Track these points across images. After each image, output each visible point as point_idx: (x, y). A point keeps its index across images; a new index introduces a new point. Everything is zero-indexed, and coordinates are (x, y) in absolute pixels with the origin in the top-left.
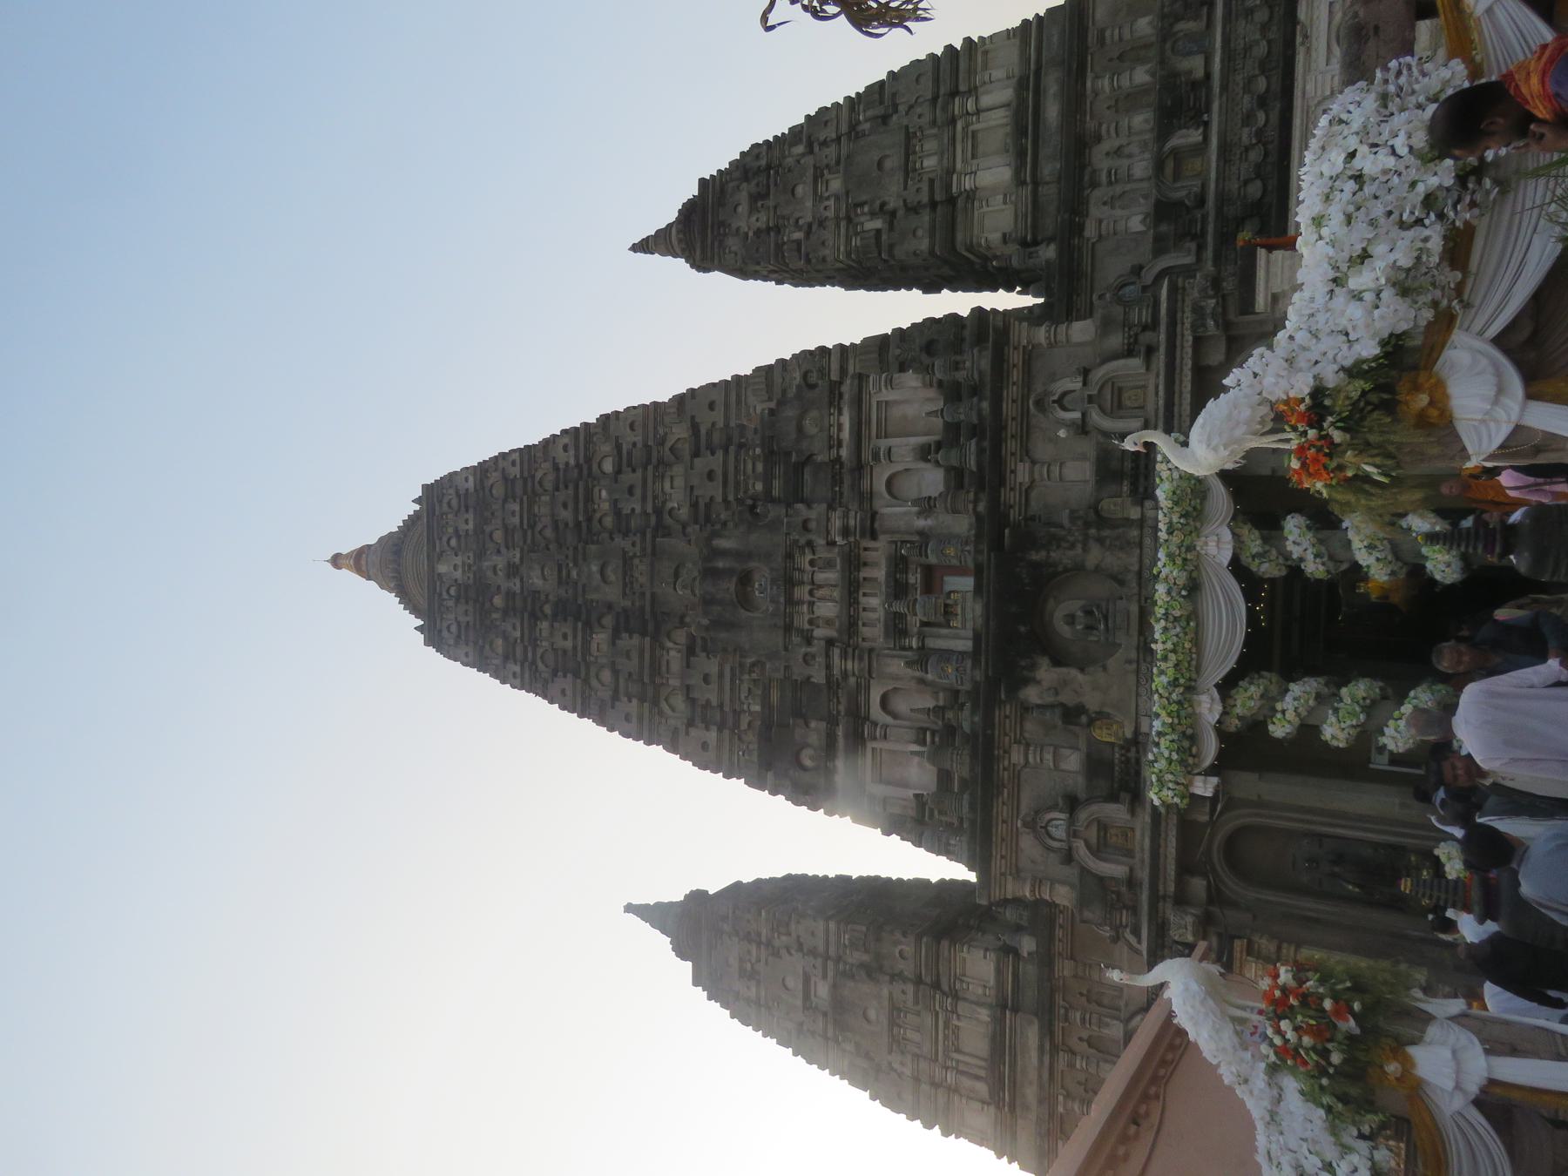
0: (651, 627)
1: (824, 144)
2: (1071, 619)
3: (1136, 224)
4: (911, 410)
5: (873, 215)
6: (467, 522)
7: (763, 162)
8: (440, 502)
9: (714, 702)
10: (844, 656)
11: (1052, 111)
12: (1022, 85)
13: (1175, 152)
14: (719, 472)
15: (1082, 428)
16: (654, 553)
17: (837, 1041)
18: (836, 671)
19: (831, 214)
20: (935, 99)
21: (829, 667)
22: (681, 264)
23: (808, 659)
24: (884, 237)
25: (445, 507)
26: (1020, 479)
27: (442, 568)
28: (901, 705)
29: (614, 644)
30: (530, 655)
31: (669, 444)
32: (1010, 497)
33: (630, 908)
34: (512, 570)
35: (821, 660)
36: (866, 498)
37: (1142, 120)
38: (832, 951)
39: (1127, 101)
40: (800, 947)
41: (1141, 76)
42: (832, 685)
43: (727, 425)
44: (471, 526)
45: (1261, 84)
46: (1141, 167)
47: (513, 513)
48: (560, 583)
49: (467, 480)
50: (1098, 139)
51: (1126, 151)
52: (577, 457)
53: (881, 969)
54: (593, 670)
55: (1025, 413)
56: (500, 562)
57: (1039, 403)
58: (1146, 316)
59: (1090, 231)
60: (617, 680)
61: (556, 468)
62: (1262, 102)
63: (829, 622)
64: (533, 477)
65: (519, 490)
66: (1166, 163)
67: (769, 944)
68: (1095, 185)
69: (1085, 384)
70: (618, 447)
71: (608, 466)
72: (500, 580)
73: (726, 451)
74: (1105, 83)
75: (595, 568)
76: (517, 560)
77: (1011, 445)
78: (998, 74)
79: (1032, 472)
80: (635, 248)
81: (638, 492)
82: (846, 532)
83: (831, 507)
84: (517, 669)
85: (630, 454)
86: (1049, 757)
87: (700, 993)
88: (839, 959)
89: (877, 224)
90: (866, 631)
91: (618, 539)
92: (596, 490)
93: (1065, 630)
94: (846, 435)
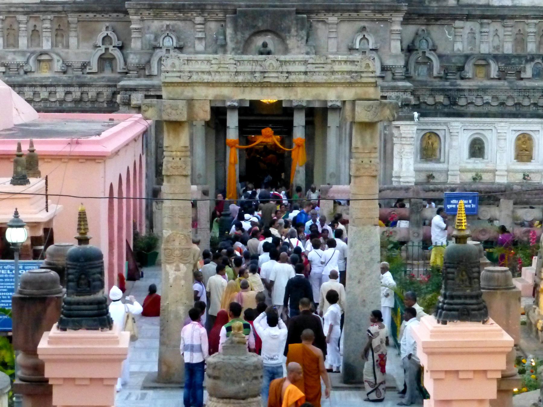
2: (265, 45)
3: (459, 46)
13: (488, 65)
26: (330, 19)
32: (322, 16)
37: (508, 48)
45: (510, 103)
46: (485, 49)
51: (496, 39)
55: (361, 20)
57: (364, 28)
58: (398, 76)
59: (458, 23)
62: (502, 104)
69: (371, 50)
77: (346, 15)
79: (333, 24)
86: (200, 35)
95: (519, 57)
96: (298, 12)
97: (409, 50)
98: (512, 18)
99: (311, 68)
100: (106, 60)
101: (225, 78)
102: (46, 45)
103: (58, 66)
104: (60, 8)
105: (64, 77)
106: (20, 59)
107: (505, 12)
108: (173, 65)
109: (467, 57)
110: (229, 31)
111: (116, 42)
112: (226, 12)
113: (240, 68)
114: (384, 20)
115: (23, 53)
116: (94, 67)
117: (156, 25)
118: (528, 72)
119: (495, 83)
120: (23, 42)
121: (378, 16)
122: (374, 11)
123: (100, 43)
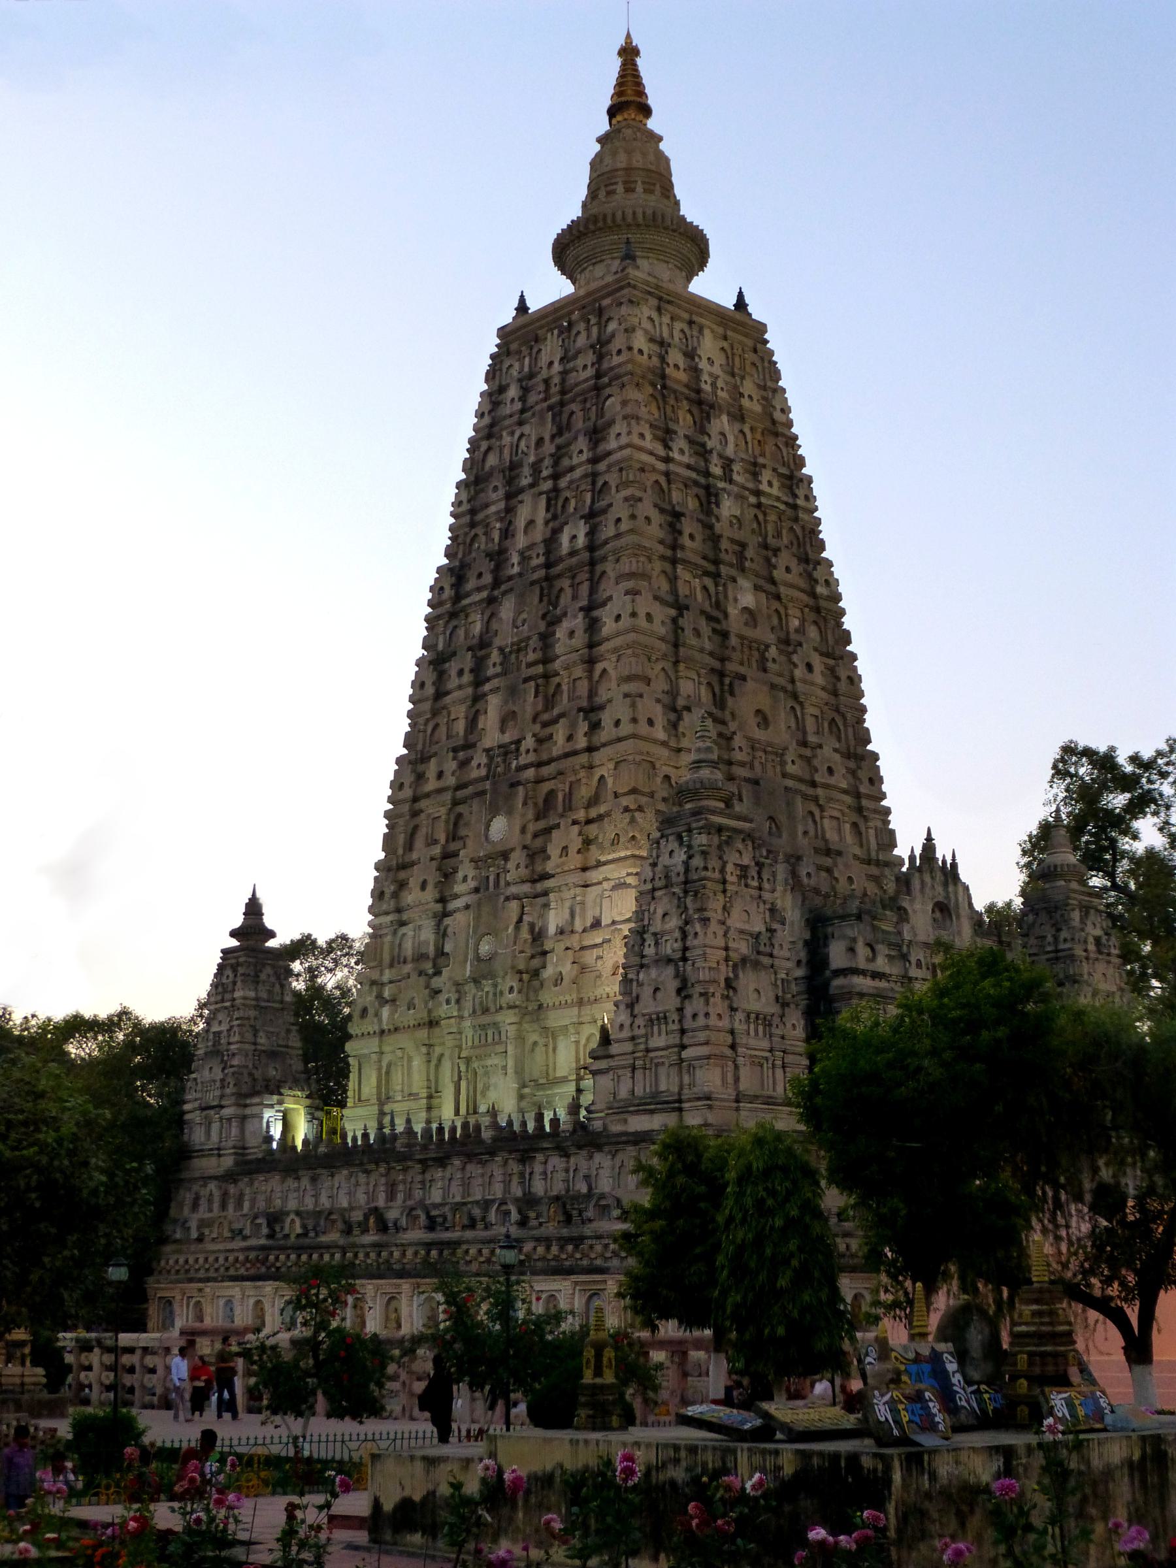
14: (832, 781)
17: (727, 959)
30: (661, 466)
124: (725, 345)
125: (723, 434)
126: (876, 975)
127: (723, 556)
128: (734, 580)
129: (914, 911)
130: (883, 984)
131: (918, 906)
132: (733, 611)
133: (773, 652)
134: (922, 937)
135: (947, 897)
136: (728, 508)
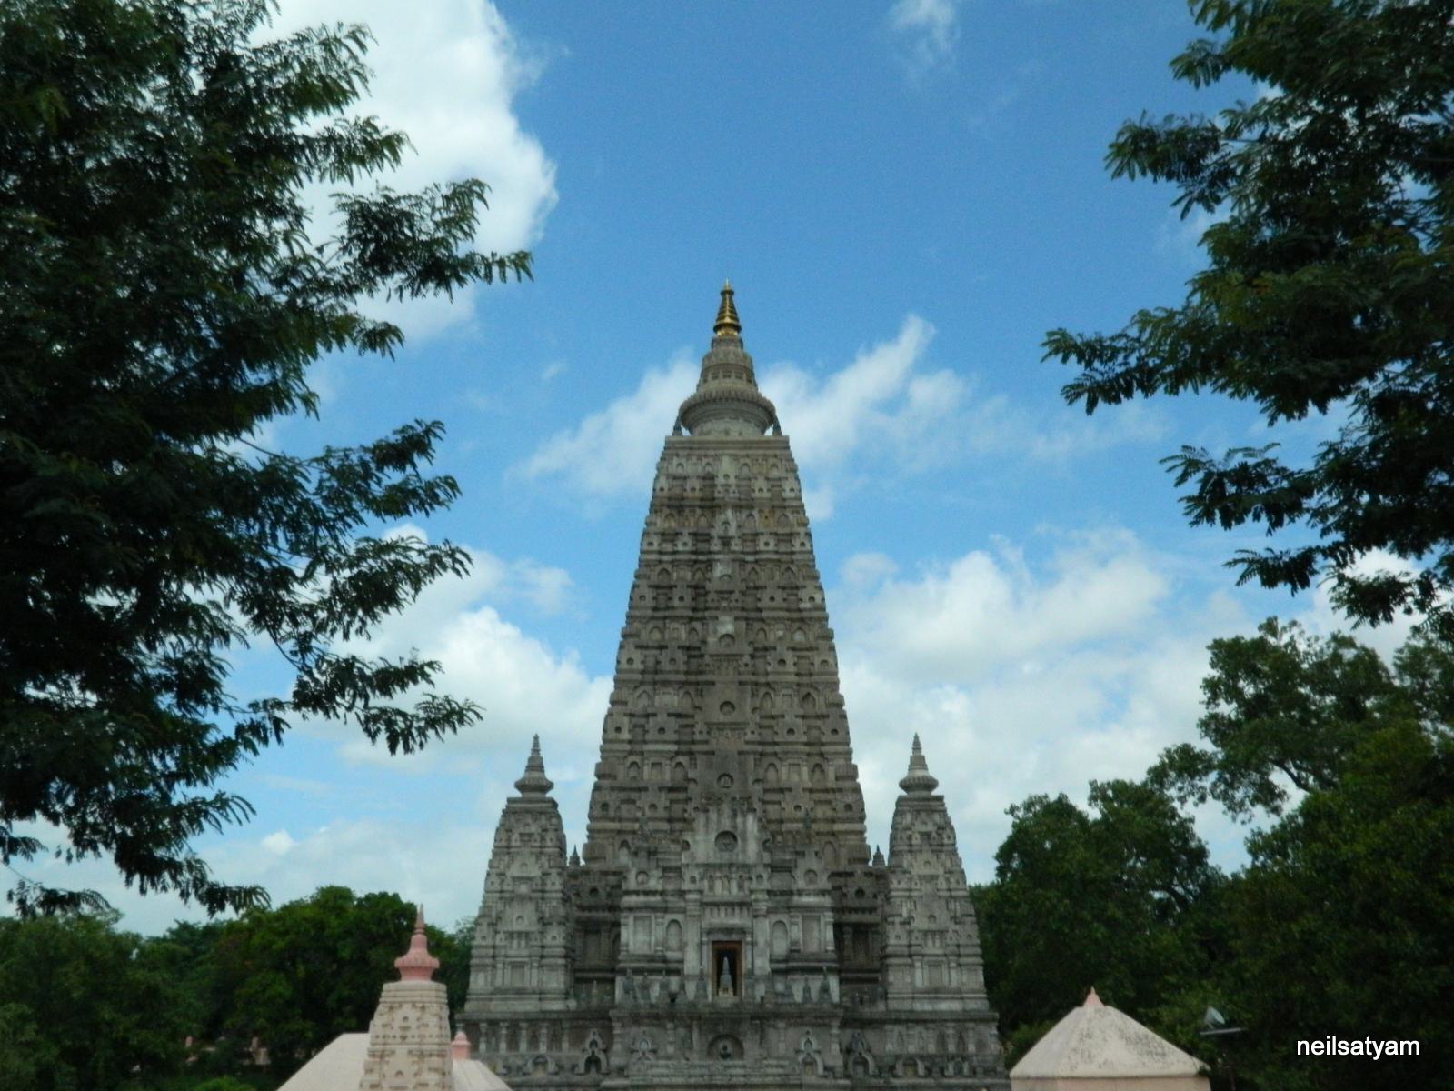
0: (692, 678)
1: (948, 880)
2: (725, 1048)
3: (889, 1047)
4: (816, 933)
5: (910, 911)
6: (761, 490)
7: (946, 841)
8: (776, 456)
9: (648, 737)
10: (696, 901)
11: (944, 1006)
12: (959, 991)
13: (916, 1064)
14: (791, 738)
15: (798, 1052)
16: (741, 683)
17: (501, 898)
18: (689, 896)
19: (913, 887)
20: (958, 946)
21: (690, 891)
22: (903, 773)
23: (693, 880)
24: (897, 920)
25: (771, 461)
27: (726, 460)
28: (674, 929)
29: (679, 647)
30: (666, 558)
31: (812, 691)
33: (536, 738)
34: (726, 541)
35: (692, 887)
36: (770, 911)
37: (932, 1048)
38: (546, 895)
39: (942, 1040)
40: (544, 874)
41: (952, 1048)
42: (682, 893)
43: (823, 744)
44: (757, 495)
46: (912, 1049)
47: (767, 544)
48: (717, 592)
49: (792, 490)
50: (927, 1029)
52: (805, 610)
53: (544, 924)
54: (660, 623)
56: (733, 531)
59: (888, 1027)
60: (653, 648)
61: (797, 588)
63: (711, 888)
64: (792, 562)
65: (783, 548)
66: (911, 1062)
67: (541, 853)
68: (908, 1028)
70: (811, 649)
71: (799, 637)
72: (717, 531)
73: (807, 744)
74: (951, 1032)
75: (729, 628)
76: (734, 548)
78: (965, 979)
80: (916, 738)
81: (780, 669)
82: (756, 900)
83: (769, 892)
84: (655, 547)
85: (808, 658)
86: (671, 1039)
87: (503, 804)
88: (543, 899)
89: (905, 913)
90: (708, 911)
91: (749, 650)
92: (782, 626)
93: (721, 1045)
94: (806, 900)
95: (941, 1056)
96: (752, 1018)
97: (847, 1051)
98: (933, 1021)
99: (749, 1071)
100: (592, 1062)
101: (680, 1080)
102: (543, 1049)
103: (551, 1067)
104: (555, 1016)
105: (557, 1079)
106: (519, 1062)
107: (927, 1017)
108: (639, 1070)
109: (897, 1057)
110: (695, 1035)
111: (601, 1046)
112: (692, 1018)
113: (692, 1072)
114: (825, 1025)
115: (523, 1056)
116: (582, 1068)
117: (634, 1031)
118: (951, 1070)
119: (923, 1081)
120: (523, 1046)
121: (820, 1021)
122: (816, 1018)
123: (587, 1045)
124: (748, 461)
125: (726, 523)
126: (647, 893)
127: (710, 604)
128: (717, 618)
129: (695, 842)
130: (652, 899)
131: (700, 837)
132: (712, 640)
133: (747, 659)
134: (701, 858)
135: (735, 827)
136: (719, 570)
